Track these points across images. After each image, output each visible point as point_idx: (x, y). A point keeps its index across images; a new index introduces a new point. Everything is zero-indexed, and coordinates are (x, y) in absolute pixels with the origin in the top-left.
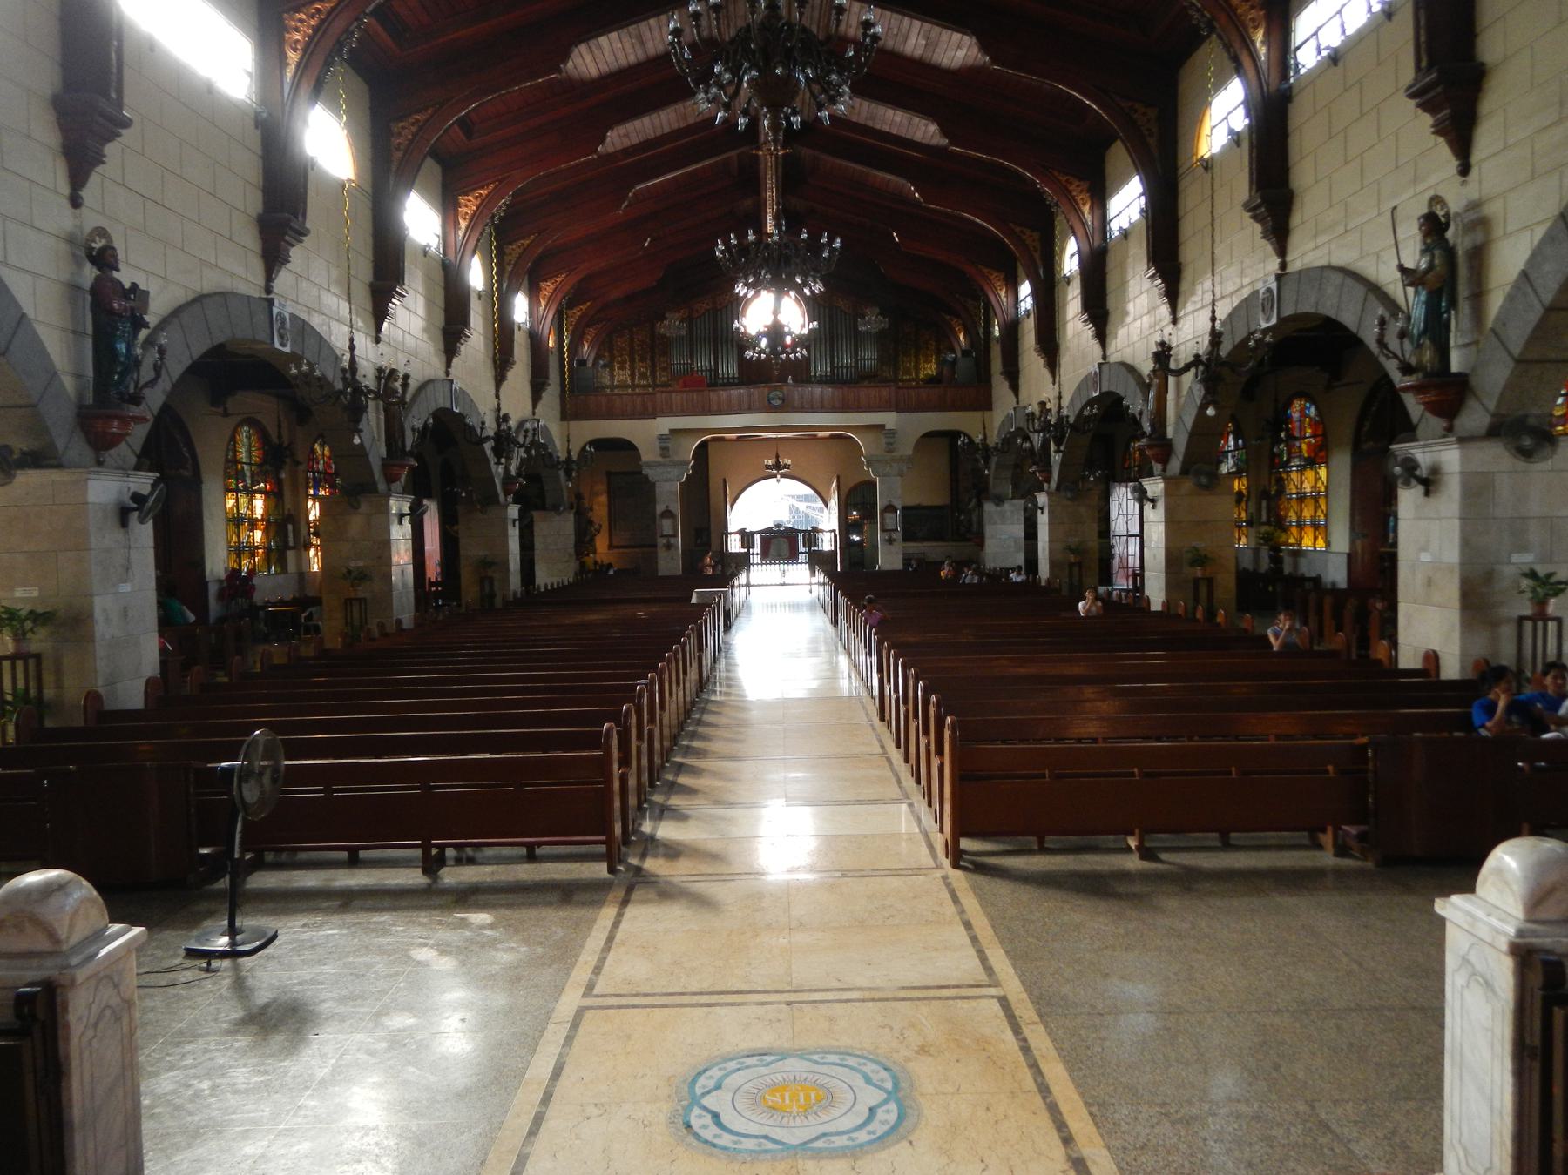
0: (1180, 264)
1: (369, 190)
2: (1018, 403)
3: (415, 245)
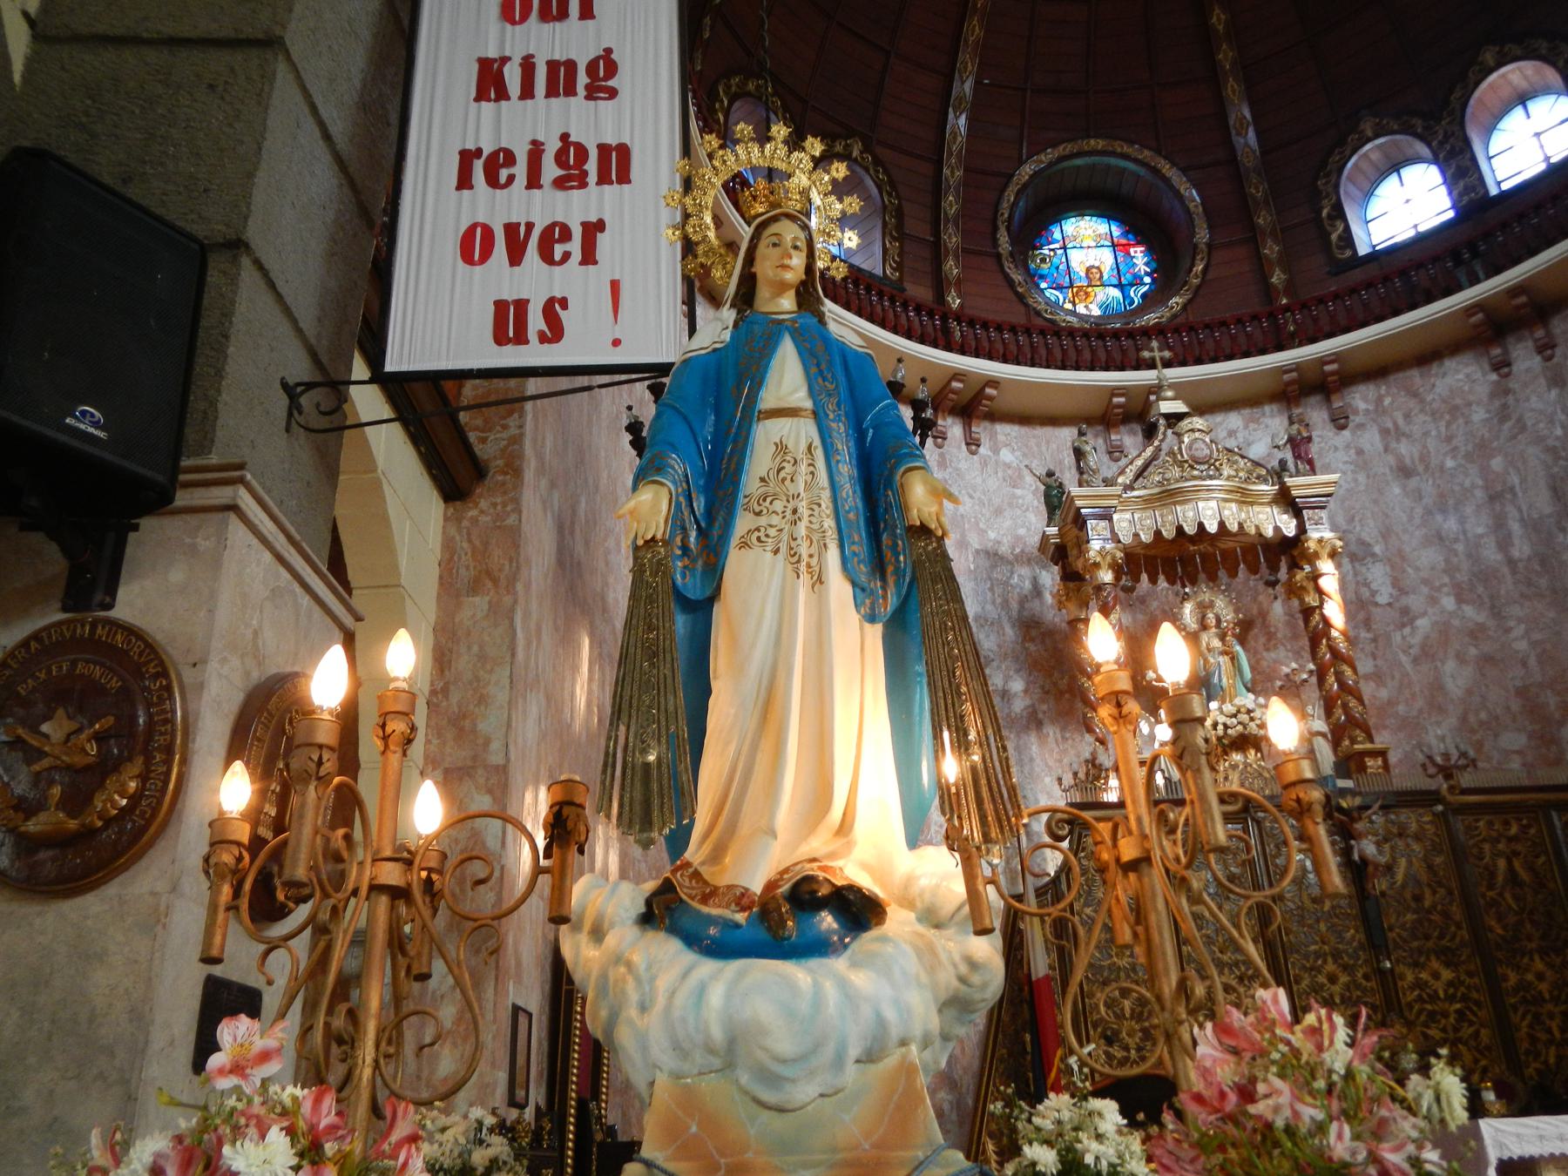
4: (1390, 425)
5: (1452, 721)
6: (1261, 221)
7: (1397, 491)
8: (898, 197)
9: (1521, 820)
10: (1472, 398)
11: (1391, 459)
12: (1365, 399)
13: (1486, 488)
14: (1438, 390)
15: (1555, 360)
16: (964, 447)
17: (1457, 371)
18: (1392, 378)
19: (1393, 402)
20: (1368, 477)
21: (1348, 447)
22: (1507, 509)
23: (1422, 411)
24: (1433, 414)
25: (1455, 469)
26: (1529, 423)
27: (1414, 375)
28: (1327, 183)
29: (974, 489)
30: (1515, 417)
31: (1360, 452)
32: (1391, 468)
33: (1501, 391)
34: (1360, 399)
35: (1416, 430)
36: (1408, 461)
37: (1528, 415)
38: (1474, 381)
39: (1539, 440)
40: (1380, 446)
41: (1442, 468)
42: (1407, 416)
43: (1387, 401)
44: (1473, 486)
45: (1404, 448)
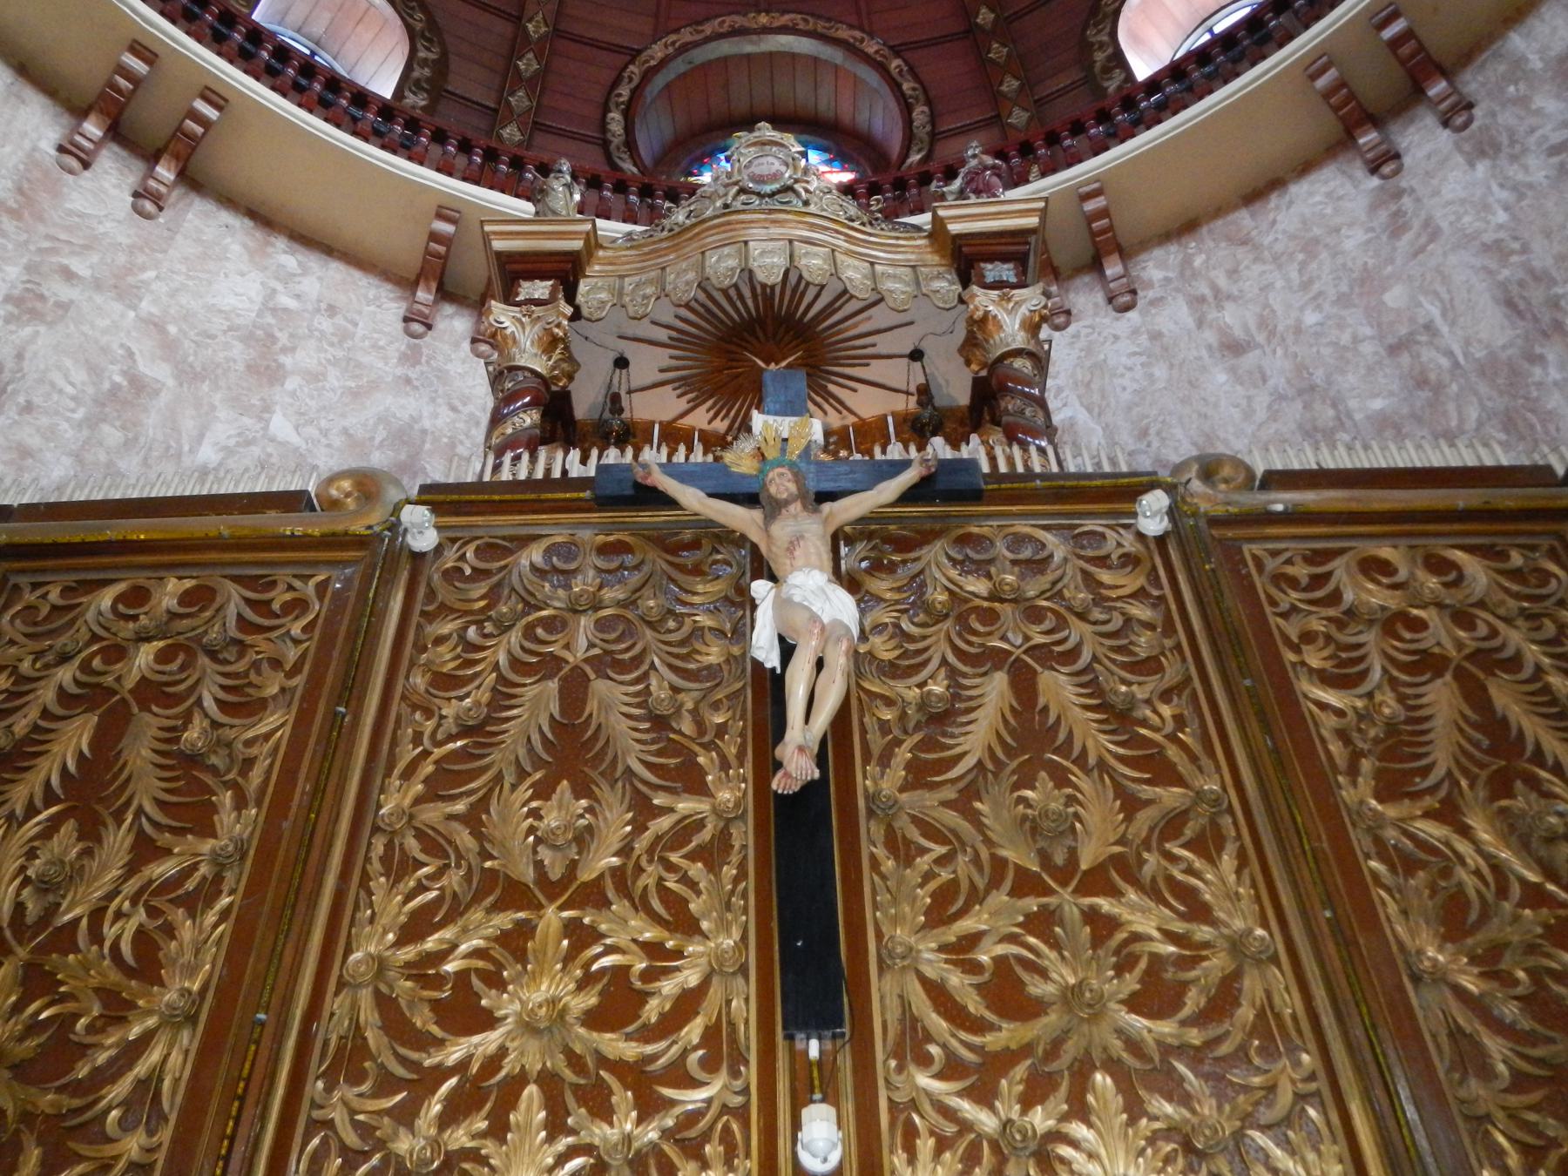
4: (1204, 289)
6: (1004, 88)
7: (1222, 377)
8: (442, 44)
9: (1503, 556)
10: (1338, 220)
11: (1210, 336)
12: (1162, 265)
13: (1381, 337)
14: (1279, 227)
15: (1475, 126)
16: (466, 345)
17: (1311, 194)
18: (1204, 230)
19: (1208, 259)
20: (1171, 366)
21: (1135, 332)
22: (1424, 359)
23: (1256, 260)
24: (1276, 258)
25: (1321, 324)
26: (1444, 225)
27: (1243, 218)
28: (1100, 31)
29: (466, 400)
30: (1416, 224)
31: (1156, 336)
32: (1209, 348)
34: (1155, 268)
35: (1249, 286)
36: (1238, 333)
37: (1438, 214)
38: (1340, 198)
39: (1466, 239)
40: (1190, 322)
41: (1298, 330)
42: (1233, 273)
43: (1198, 261)
44: (1356, 340)
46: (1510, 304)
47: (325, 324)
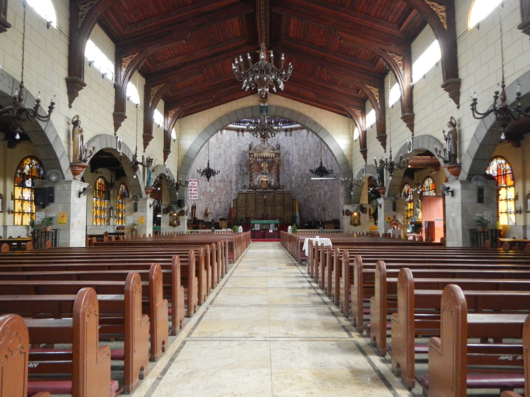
0: (460, 80)
1: (68, 36)
2: (366, 163)
3: (97, 71)
5: (294, 177)
33: (307, 136)
34: (294, 132)
45: (297, 141)
46: (309, 151)
47: (233, 138)
